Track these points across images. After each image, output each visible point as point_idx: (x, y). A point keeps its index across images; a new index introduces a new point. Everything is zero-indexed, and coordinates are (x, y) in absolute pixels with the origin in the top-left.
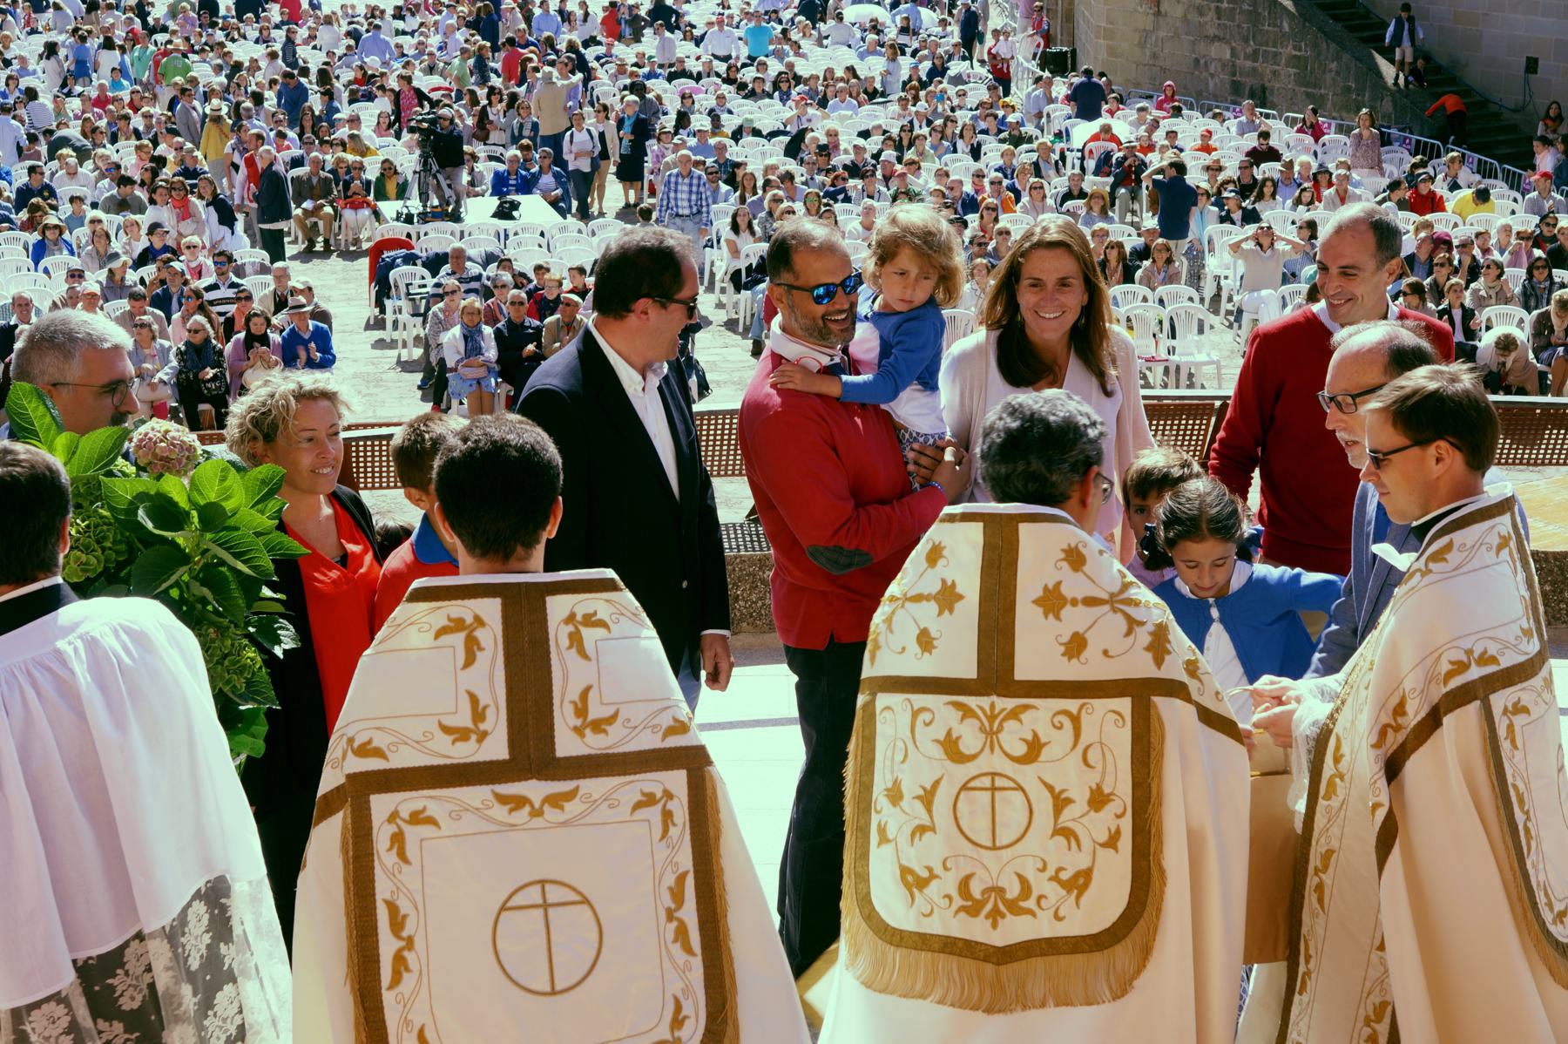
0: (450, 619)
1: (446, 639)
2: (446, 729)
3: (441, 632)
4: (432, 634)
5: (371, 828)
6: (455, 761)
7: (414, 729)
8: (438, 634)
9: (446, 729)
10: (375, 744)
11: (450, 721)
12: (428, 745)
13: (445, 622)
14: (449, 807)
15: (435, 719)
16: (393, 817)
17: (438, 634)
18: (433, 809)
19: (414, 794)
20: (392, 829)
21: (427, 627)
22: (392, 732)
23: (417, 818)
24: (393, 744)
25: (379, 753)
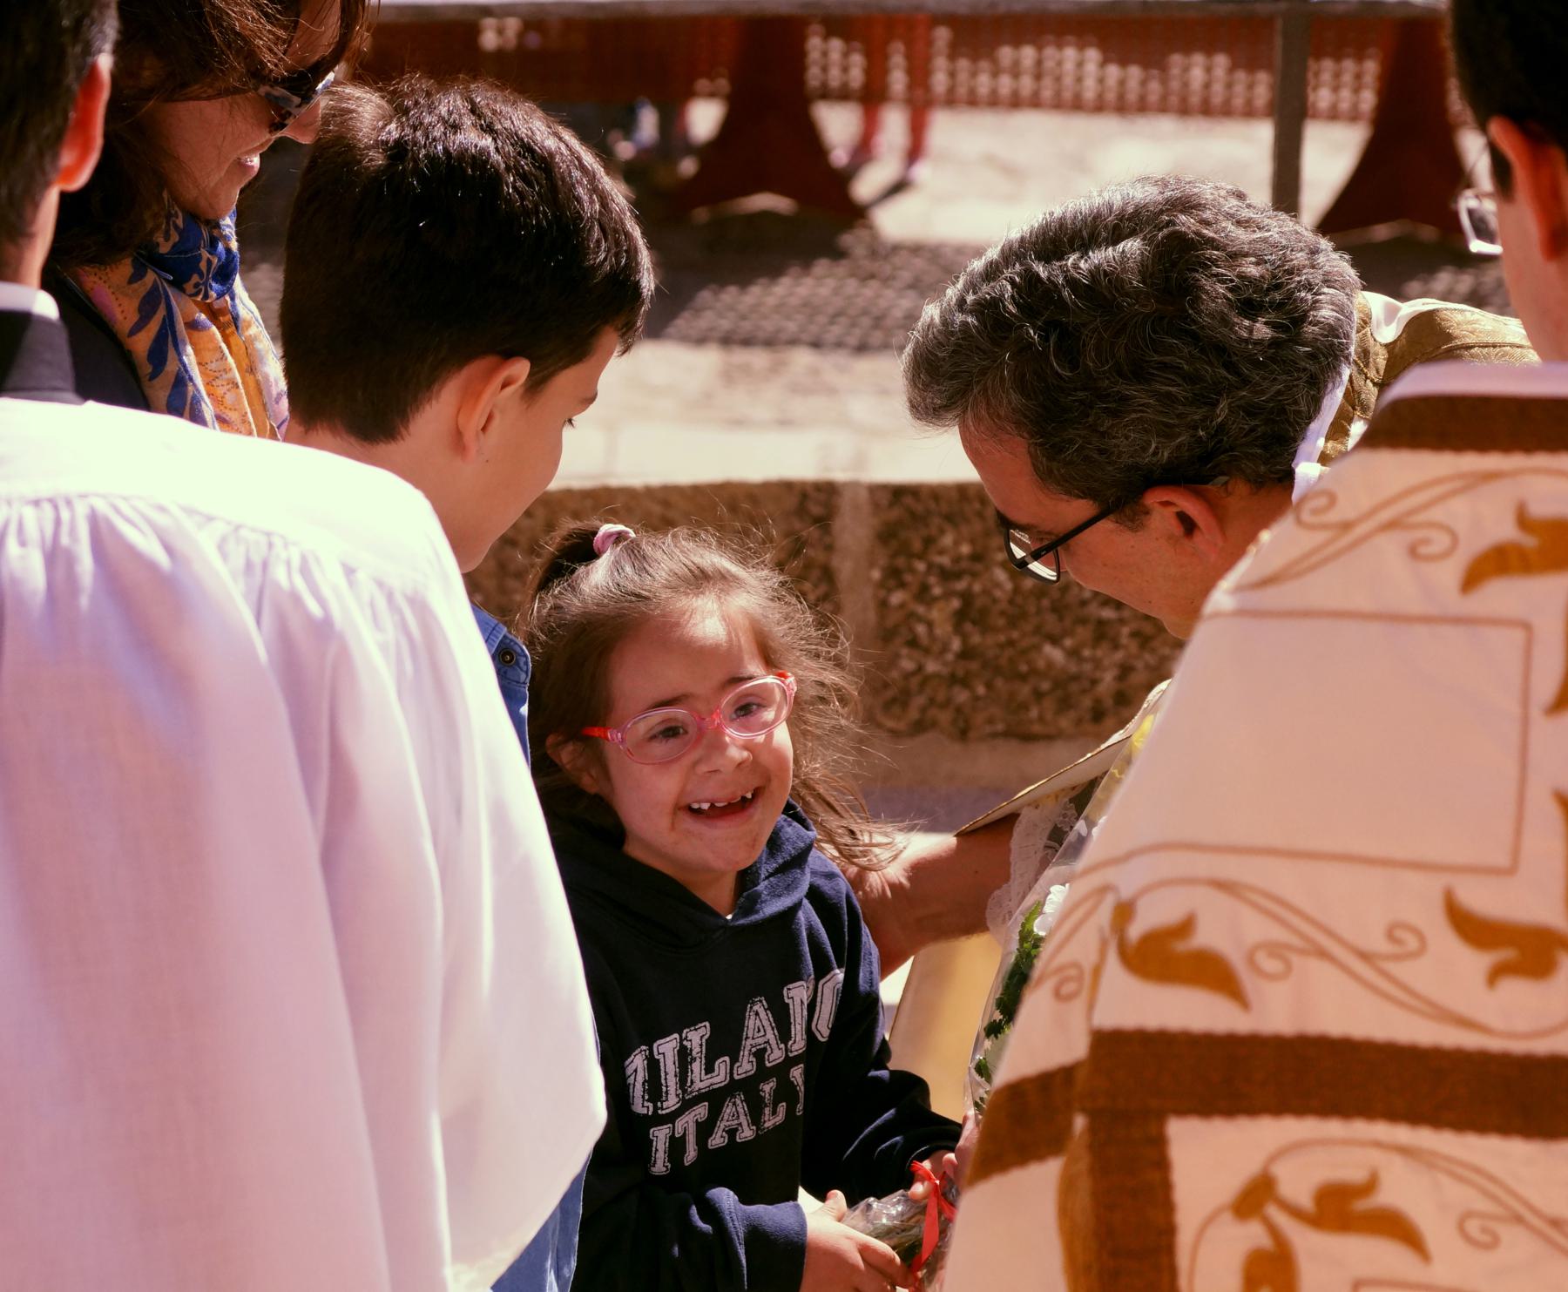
0: (1524, 520)
1: (1503, 595)
2: (1471, 928)
3: (1495, 563)
4: (1449, 573)
5: (1168, 1231)
6: (1495, 1044)
7: (1360, 907)
8: (1473, 578)
9: (1471, 928)
10: (1207, 937)
11: (1483, 899)
12: (1393, 968)
13: (1504, 530)
14: (1462, 1196)
15: (1432, 887)
16: (1255, 1197)
17: (1473, 578)
18: (1402, 1189)
19: (1334, 1128)
20: (1252, 1235)
21: (1441, 541)
22: (1273, 905)
23: (1340, 1208)
24: (1275, 949)
25: (1212, 973)
